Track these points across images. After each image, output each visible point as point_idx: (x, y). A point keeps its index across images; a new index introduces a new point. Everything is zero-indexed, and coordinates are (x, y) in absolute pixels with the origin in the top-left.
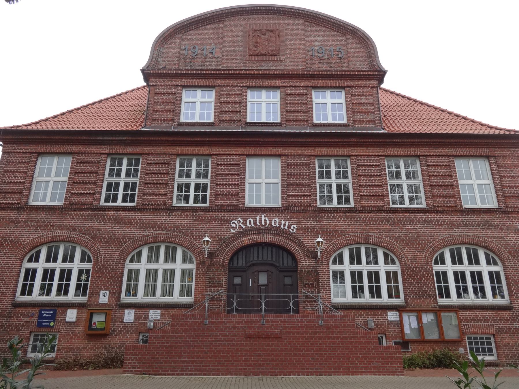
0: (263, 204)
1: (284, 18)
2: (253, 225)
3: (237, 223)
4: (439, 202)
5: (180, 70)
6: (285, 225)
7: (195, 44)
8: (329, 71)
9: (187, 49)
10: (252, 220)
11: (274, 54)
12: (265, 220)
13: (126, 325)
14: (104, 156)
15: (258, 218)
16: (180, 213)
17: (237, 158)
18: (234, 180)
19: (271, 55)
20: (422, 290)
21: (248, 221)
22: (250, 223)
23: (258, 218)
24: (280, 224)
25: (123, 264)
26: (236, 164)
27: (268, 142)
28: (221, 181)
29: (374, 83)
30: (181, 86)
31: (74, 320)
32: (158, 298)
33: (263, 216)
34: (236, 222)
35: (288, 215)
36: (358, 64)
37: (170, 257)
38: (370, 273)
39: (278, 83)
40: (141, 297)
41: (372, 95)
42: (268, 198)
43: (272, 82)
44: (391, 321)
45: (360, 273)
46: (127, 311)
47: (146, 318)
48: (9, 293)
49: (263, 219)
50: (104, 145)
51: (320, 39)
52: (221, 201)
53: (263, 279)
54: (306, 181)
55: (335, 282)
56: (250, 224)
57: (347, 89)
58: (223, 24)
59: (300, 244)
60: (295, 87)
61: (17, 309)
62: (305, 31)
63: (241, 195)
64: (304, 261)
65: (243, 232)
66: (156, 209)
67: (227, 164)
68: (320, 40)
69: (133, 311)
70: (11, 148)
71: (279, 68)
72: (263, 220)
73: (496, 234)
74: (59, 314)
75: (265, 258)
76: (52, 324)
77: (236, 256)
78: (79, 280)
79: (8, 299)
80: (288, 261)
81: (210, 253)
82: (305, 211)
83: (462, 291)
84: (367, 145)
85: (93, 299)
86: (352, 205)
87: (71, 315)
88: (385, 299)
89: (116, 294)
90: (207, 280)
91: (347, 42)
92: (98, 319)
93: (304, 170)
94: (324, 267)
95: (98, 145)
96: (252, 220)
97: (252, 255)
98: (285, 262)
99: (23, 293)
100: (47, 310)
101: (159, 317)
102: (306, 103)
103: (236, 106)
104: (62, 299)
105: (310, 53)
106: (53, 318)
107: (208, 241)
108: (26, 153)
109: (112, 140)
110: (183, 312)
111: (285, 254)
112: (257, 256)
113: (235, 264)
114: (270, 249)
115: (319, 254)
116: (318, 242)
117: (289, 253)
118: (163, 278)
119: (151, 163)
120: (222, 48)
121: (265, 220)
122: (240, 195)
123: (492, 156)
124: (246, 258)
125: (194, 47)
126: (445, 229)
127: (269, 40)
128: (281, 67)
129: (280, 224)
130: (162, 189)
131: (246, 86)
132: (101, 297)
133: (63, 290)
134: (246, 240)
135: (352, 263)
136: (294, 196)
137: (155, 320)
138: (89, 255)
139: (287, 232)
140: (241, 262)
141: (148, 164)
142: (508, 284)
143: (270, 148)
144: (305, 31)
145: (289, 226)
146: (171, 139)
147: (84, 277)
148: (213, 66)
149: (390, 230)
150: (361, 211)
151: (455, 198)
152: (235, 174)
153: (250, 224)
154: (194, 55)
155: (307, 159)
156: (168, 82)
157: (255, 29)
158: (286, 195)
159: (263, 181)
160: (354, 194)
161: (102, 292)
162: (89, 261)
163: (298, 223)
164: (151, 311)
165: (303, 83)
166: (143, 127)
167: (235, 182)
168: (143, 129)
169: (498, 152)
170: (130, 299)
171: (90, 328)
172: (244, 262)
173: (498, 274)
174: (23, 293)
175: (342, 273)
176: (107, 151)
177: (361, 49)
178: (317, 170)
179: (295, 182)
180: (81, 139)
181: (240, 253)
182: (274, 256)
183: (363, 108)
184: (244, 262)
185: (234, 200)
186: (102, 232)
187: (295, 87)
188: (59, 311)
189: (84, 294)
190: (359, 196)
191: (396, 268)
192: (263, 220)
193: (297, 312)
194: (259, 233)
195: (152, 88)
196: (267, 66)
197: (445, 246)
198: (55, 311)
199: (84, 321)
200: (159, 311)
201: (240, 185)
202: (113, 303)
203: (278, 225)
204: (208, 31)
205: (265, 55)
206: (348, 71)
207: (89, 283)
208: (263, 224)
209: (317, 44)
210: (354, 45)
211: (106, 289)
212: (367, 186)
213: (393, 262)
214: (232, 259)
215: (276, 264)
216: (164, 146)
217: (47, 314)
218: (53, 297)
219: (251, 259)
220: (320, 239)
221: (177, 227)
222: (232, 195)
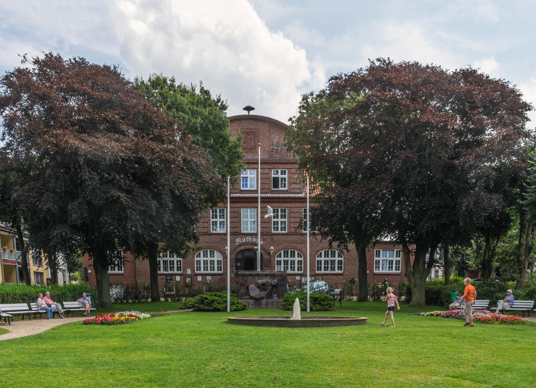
0: (249, 231)
13: (199, 282)
17: (237, 209)
22: (244, 240)
32: (209, 272)
40: (202, 271)
47: (206, 279)
51: (277, 137)
55: (277, 265)
65: (241, 245)
74: (173, 278)
78: (177, 265)
82: (267, 235)
84: (295, 202)
86: (286, 232)
89: (193, 270)
92: (188, 280)
94: (273, 259)
102: (269, 179)
105: (272, 147)
106: (171, 279)
133: (172, 268)
144: (269, 132)
147: (179, 263)
150: (290, 235)
165: (268, 166)
175: (280, 261)
188: (173, 277)
197: (322, 250)
199: (182, 281)
202: (193, 274)
209: (275, 140)
218: (170, 272)
220: (272, 248)
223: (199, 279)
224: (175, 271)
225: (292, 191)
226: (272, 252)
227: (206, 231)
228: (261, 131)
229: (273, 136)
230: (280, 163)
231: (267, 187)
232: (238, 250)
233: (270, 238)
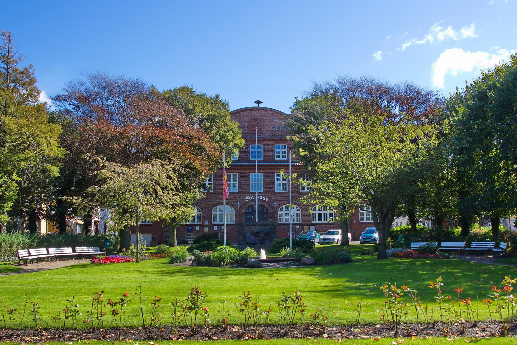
38: (324, 213)
45: (321, 213)
54: (272, 183)
62: (272, 118)
64: (270, 210)
87: (197, 228)
89: (210, 222)
93: (271, 178)
110: (232, 226)
163: (268, 198)
170: (215, 223)
173: (300, 214)
185: (247, 190)
188: (194, 227)
191: (300, 212)
223: (215, 228)
224: (196, 223)
229: (275, 121)
232: (248, 205)
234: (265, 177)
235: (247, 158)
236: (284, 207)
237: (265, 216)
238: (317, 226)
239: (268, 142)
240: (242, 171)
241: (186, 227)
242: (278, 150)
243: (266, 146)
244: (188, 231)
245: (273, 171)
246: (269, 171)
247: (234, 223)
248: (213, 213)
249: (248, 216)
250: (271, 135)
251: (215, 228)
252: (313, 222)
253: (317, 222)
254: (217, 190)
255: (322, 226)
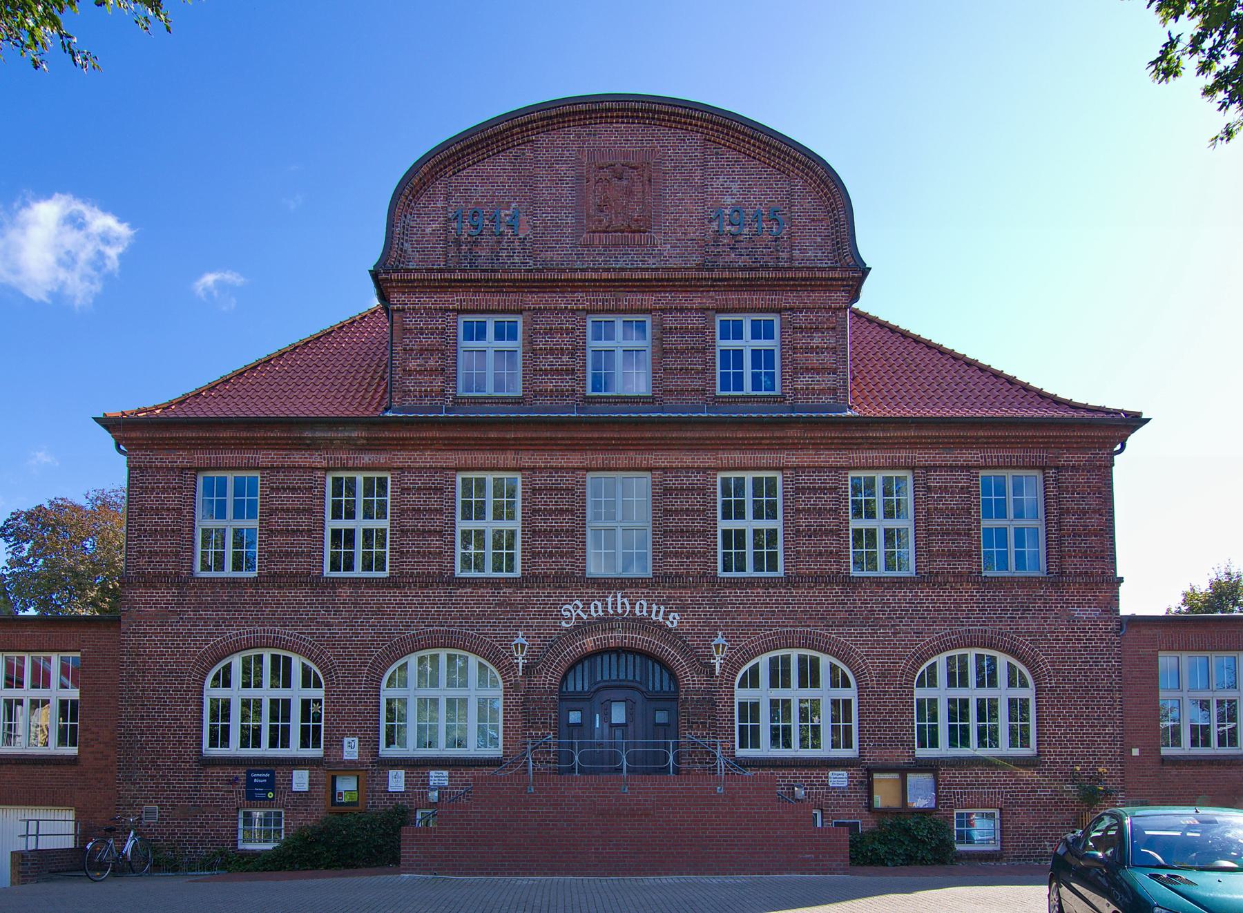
0: (619, 572)
1: (661, 132)
2: (602, 614)
3: (572, 611)
4: (940, 564)
5: (450, 271)
6: (658, 612)
7: (477, 203)
8: (752, 269)
9: (459, 219)
10: (599, 604)
11: (639, 228)
12: (623, 604)
14: (319, 473)
15: (610, 600)
16: (469, 590)
18: (565, 522)
19: (634, 232)
20: (886, 724)
21: (592, 606)
23: (610, 600)
24: (649, 612)
25: (378, 689)
26: (567, 489)
27: (628, 439)
28: (541, 525)
29: (838, 297)
30: (454, 310)
31: (306, 788)
32: (442, 750)
33: (619, 595)
34: (570, 607)
35: (665, 594)
36: (810, 251)
37: (458, 677)
39: (649, 300)
41: (834, 328)
42: (628, 559)
43: (636, 299)
44: (834, 788)
46: (392, 773)
47: (426, 784)
48: (190, 741)
49: (619, 602)
50: (317, 450)
52: (542, 566)
53: (618, 714)
54: (698, 525)
56: (596, 611)
57: (786, 315)
58: (534, 150)
59: (686, 649)
60: (681, 310)
61: (210, 771)
62: (704, 166)
63: (578, 553)
64: (691, 680)
65: (583, 628)
66: (426, 581)
67: (551, 489)
68: (735, 191)
69: (402, 773)
70: (145, 457)
71: (651, 262)
72: (618, 603)
73: (1034, 627)
74: (279, 779)
75: (622, 676)
76: (270, 795)
77: (571, 674)
79: (191, 752)
80: (662, 681)
81: (527, 668)
83: (959, 736)
85: (333, 752)
88: (825, 750)
89: (370, 744)
90: (525, 708)
91: (790, 194)
93: (695, 501)
95: (306, 450)
96: (599, 604)
97: (599, 668)
98: (659, 682)
99: (213, 744)
100: (260, 772)
101: (446, 783)
103: (565, 358)
104: (279, 752)
105: (714, 226)
106: (270, 785)
107: (523, 646)
108: (172, 468)
109: (332, 440)
110: (486, 771)
111: (657, 668)
112: (608, 670)
113: (571, 689)
114: (631, 658)
115: (718, 666)
116: (717, 646)
117: (664, 665)
118: (450, 709)
119: (408, 489)
120: (533, 215)
121: (623, 604)
122: (577, 553)
123: (1050, 468)
124: (590, 672)
125: (475, 214)
126: (945, 619)
127: (629, 193)
128: (654, 261)
129: (649, 612)
130: (434, 543)
131: (583, 310)
132: (346, 748)
133: (280, 737)
134: (589, 643)
135: (774, 684)
136: (676, 554)
137: (440, 788)
138: (316, 675)
139: (661, 626)
140: (579, 683)
141: (403, 489)
142: (1039, 721)
143: (632, 454)
144: (704, 166)
145: (666, 614)
146: (443, 435)
148: (516, 262)
149: (846, 622)
151: (970, 556)
152: (567, 510)
153: (596, 611)
154: (475, 232)
155: (700, 476)
156: (428, 300)
157: (601, 162)
158: (661, 554)
159: (620, 515)
160: (786, 549)
161: (346, 740)
162: (318, 684)
163: (682, 609)
164: (432, 773)
166: (386, 410)
167: (567, 527)
168: (388, 414)
169: (1066, 458)
171: (334, 803)
172: (586, 685)
174: (213, 744)
176: (325, 464)
177: (819, 215)
178: (720, 499)
179: (676, 519)
180: (273, 438)
181: (579, 667)
182: (638, 672)
183: (814, 360)
184: (586, 685)
186: (335, 629)
187: (681, 310)
188: (280, 773)
189: (317, 744)
190: (793, 555)
192: (618, 603)
193: (677, 771)
194: (613, 629)
195: (396, 316)
196: (625, 260)
198: (272, 773)
199: (322, 792)
200: (446, 773)
201: (577, 532)
202: (368, 759)
203: (645, 613)
204: (499, 168)
205: (622, 232)
206: (790, 269)
207: (322, 724)
208: (620, 611)
209: (729, 200)
210: (806, 203)
211: (354, 735)
212: (811, 534)
213: (846, 684)
214: (565, 677)
215: (639, 686)
216: (432, 450)
217: (258, 778)
219: (599, 678)
221: (467, 618)
222: (562, 555)
223: (397, 781)
224: (295, 749)
225: (801, 400)
226: (717, 662)
227: (433, 568)
228: (669, 166)
229: (718, 183)
230: (751, 285)
231: (696, 384)
233: (712, 602)
234: (662, 493)
235: (566, 383)
236: (763, 661)
237: (661, 717)
238: (945, 775)
239: (680, 299)
240: (540, 459)
241: (241, 773)
242: (731, 344)
243: (670, 320)
244: (250, 796)
245: (705, 459)
246: (688, 459)
247: (496, 752)
248: (386, 693)
249: (574, 717)
250: (695, 260)
251: (397, 781)
252: (921, 753)
253: (943, 749)
254: (408, 565)
255: (971, 774)
